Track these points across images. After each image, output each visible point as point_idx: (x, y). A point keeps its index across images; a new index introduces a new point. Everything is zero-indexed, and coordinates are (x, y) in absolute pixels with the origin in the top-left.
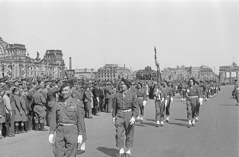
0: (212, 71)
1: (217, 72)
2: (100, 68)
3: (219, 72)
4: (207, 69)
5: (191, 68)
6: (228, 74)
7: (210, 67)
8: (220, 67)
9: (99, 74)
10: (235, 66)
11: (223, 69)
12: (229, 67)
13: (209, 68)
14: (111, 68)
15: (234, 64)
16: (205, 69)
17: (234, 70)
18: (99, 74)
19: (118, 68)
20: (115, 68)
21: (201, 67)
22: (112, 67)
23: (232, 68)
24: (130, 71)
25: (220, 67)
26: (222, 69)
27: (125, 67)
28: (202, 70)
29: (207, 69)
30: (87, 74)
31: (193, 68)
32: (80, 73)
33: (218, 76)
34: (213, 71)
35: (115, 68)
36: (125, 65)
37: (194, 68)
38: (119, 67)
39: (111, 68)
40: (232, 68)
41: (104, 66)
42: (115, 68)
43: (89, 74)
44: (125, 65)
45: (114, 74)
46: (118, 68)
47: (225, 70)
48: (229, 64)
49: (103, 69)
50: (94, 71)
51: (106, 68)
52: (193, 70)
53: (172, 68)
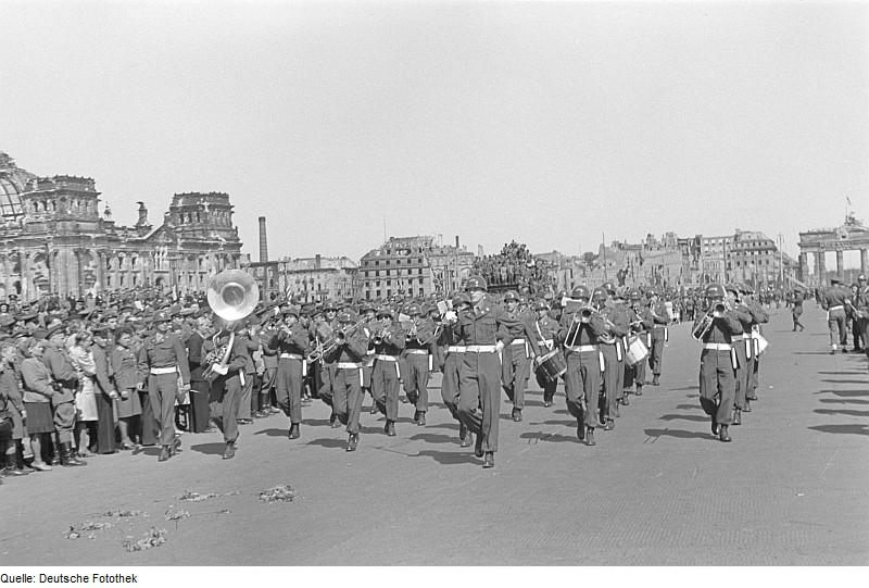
0: (775, 249)
1: (794, 253)
4: (757, 244)
5: (698, 240)
8: (800, 234)
9: (367, 274)
10: (857, 227)
11: (815, 241)
12: (833, 234)
14: (409, 252)
15: (851, 221)
16: (747, 242)
17: (852, 244)
18: (367, 274)
21: (736, 237)
22: (412, 245)
23: (843, 237)
25: (800, 234)
27: (461, 247)
28: (739, 245)
29: (757, 244)
30: (322, 275)
31: (706, 242)
32: (297, 272)
36: (457, 237)
37: (710, 239)
38: (437, 247)
39: (409, 252)
40: (843, 237)
41: (383, 244)
43: (330, 275)
44: (457, 237)
47: (818, 245)
48: (835, 222)
49: (378, 254)
50: (348, 265)
51: (389, 252)
52: (707, 249)
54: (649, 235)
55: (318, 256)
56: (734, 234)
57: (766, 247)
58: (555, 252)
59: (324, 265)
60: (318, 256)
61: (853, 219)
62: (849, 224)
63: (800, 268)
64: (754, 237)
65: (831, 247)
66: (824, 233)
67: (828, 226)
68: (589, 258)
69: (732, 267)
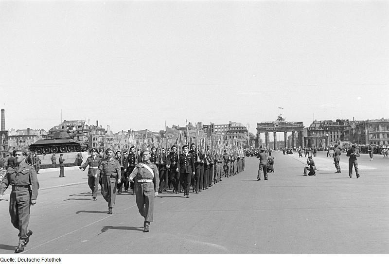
0: (247, 131)
2: (53, 127)
5: (212, 126)
6: (271, 134)
7: (244, 124)
10: (283, 121)
11: (263, 127)
12: (272, 124)
13: (242, 126)
17: (280, 130)
19: (85, 128)
20: (79, 127)
21: (229, 125)
23: (277, 126)
24: (106, 132)
26: (260, 127)
27: (99, 126)
28: (231, 129)
31: (216, 127)
34: (249, 132)
35: (81, 126)
36: (97, 121)
37: (218, 126)
38: (87, 126)
40: (277, 126)
41: (60, 123)
44: (97, 121)
45: (78, 137)
46: (85, 128)
48: (273, 119)
51: (63, 127)
52: (216, 130)
55: (29, 129)
56: (228, 124)
57: (242, 130)
58: (146, 130)
59: (32, 133)
60: (29, 129)
63: (257, 140)
64: (237, 125)
66: (268, 124)
67: (270, 121)
68: (162, 133)
69: (228, 138)
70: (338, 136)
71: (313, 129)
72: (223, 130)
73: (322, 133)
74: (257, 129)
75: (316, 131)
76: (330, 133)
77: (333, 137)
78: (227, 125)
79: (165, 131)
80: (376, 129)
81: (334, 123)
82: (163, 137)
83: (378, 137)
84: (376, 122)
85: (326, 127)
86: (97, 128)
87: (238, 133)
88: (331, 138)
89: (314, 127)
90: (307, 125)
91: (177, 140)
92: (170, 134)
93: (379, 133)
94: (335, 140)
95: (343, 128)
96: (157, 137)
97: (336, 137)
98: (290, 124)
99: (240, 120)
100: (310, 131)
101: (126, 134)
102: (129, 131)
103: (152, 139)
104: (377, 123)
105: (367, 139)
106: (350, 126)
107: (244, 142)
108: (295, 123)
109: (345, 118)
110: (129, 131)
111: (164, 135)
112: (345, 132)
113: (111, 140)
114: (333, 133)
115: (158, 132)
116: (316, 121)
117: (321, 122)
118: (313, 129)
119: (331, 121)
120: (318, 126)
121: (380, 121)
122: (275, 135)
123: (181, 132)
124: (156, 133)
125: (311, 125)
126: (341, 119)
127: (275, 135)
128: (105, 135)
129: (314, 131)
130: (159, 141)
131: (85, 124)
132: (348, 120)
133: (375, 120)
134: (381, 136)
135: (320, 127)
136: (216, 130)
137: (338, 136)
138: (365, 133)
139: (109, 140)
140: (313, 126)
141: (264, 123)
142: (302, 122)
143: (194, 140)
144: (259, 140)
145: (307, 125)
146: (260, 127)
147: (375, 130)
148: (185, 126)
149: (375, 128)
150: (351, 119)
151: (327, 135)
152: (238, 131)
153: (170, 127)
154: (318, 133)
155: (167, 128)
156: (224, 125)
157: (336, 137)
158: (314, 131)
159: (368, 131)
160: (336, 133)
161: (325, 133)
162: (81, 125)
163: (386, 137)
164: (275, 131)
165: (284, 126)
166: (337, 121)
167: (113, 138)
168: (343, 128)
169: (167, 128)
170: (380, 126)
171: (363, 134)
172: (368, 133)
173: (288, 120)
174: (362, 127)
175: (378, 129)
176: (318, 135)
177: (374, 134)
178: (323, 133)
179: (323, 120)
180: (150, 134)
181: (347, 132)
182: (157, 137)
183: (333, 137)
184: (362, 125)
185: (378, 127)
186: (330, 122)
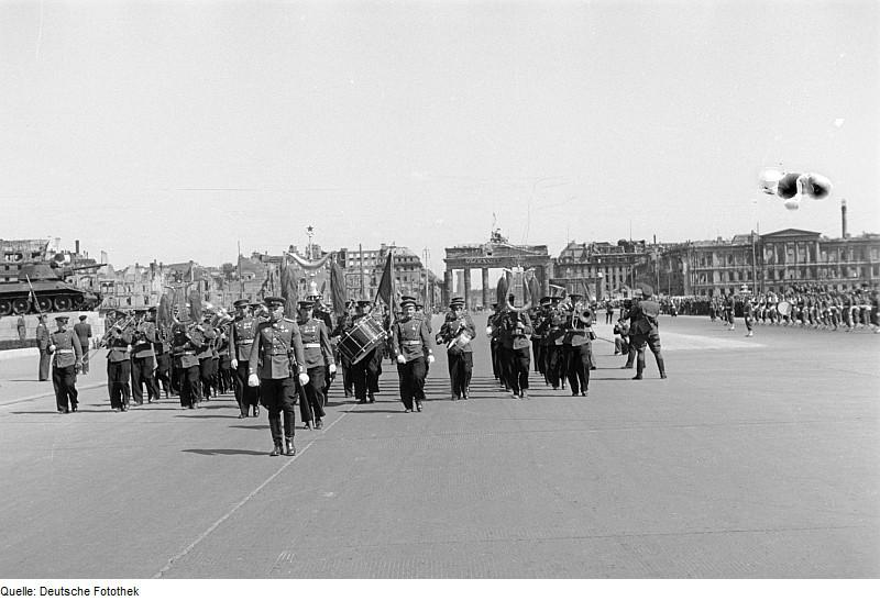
0: (420, 265)
1: (438, 269)
3: (444, 267)
5: (343, 254)
6: (476, 273)
8: (446, 250)
10: (503, 244)
11: (460, 258)
14: (20, 256)
17: (497, 263)
20: (35, 255)
21: (382, 252)
23: (490, 254)
26: (453, 256)
27: (81, 252)
31: (351, 256)
33: (440, 285)
35: (38, 254)
36: (77, 242)
38: (52, 252)
39: (20, 256)
40: (490, 254)
42: (38, 254)
44: (77, 242)
48: (479, 238)
52: (352, 263)
53: (271, 254)
54: (291, 247)
57: (411, 264)
61: (499, 236)
62: (495, 241)
64: (400, 253)
65: (476, 265)
66: (470, 249)
68: (227, 269)
70: (621, 277)
71: (568, 261)
72: (366, 263)
73: (586, 271)
74: (445, 261)
75: (573, 266)
76: (604, 270)
77: (611, 280)
78: (375, 252)
79: (235, 264)
80: (706, 260)
81: (613, 248)
82: (229, 278)
83: (711, 280)
84: (707, 245)
85: (596, 258)
86: (78, 257)
87: (402, 270)
88: (607, 280)
89: (570, 258)
90: (555, 252)
91: (265, 284)
92: (246, 273)
93: (712, 271)
94: (615, 286)
95: (632, 259)
96: (217, 279)
97: (618, 279)
98: (519, 250)
99: (407, 242)
100: (560, 266)
101: (143, 271)
102: (152, 264)
103: (206, 284)
104: (709, 248)
105: (686, 284)
106: (647, 256)
107: (416, 290)
108: (530, 248)
109: (637, 239)
110: (152, 264)
111: (234, 274)
112: (638, 267)
113: (111, 285)
114: (610, 270)
115: (218, 265)
116: (573, 243)
117: (584, 245)
118: (568, 261)
119: (607, 243)
120: (578, 254)
121: (715, 244)
122: (485, 275)
123: (272, 267)
124: (214, 269)
125: (563, 253)
126: (628, 240)
127: (485, 275)
128: (95, 273)
129: (570, 265)
130: (220, 288)
131: (49, 249)
132: (643, 242)
133: (702, 243)
134: (716, 277)
135: (584, 256)
136: (352, 263)
137: (621, 277)
138: (681, 271)
139: (105, 285)
140: (567, 255)
141: (461, 247)
142: (545, 247)
143: (303, 285)
144: (449, 285)
145: (555, 252)
146: (453, 256)
147: (703, 264)
148: (282, 255)
149: (703, 260)
150: (649, 241)
151: (600, 275)
152: (402, 265)
153: (247, 255)
154: (579, 271)
155: (241, 258)
156: (370, 252)
157: (618, 279)
158: (570, 265)
159: (688, 267)
160: (618, 269)
161: (593, 271)
162: (38, 250)
163: (728, 279)
164: (485, 266)
165: (502, 254)
166: (620, 243)
167: (116, 281)
168: (632, 259)
169: (241, 258)
170: (714, 256)
171: (678, 273)
172: (688, 270)
173: (514, 240)
174: (675, 257)
175: (710, 263)
176: (579, 276)
177: (702, 273)
178: (590, 269)
179: (589, 241)
180: (200, 271)
181: (642, 268)
182: (217, 279)
183: (611, 280)
184: (676, 253)
185: (710, 258)
186: (604, 246)
